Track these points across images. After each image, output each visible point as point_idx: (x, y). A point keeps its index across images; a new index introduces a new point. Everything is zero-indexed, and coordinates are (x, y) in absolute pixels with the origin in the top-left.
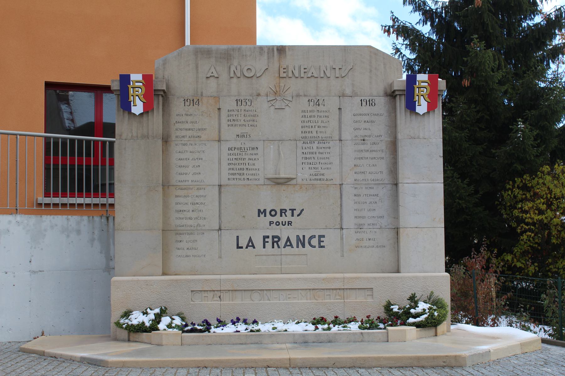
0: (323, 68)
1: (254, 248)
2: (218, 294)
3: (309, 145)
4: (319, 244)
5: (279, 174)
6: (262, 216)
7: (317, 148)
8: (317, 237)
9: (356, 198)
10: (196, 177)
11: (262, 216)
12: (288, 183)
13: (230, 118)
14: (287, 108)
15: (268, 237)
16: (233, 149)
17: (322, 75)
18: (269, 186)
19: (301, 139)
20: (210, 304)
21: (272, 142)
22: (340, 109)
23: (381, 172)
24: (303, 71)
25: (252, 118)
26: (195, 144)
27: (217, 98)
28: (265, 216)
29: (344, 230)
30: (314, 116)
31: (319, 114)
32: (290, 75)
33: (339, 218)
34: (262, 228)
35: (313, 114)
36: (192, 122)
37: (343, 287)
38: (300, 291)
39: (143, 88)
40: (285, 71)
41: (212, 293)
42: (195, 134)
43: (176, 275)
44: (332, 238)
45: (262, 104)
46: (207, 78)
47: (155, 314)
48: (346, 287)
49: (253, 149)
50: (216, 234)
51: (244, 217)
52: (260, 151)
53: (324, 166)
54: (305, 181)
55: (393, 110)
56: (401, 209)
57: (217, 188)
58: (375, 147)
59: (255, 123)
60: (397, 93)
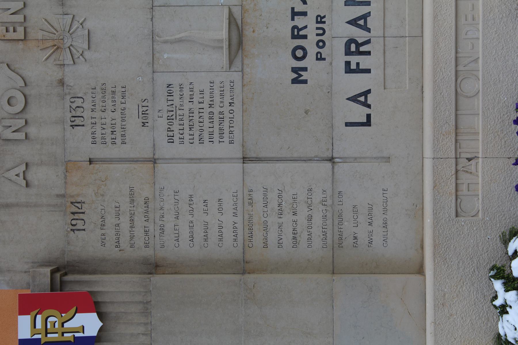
1: (369, 91)
2: (463, 162)
5: (221, 41)
6: (305, 75)
10: (228, 205)
11: (305, 75)
12: (239, 22)
13: (108, 140)
14: (88, 25)
15: (348, 64)
16: (171, 134)
18: (246, 61)
20: (483, 179)
21: (157, 55)
25: (108, 96)
26: (162, 208)
27: (69, 166)
28: (305, 69)
32: (19, 18)
34: (329, 74)
36: (118, 215)
39: (47, 312)
40: (11, 29)
41: (461, 175)
42: (141, 209)
43: (422, 247)
45: (80, 76)
46: (27, 185)
47: (507, 291)
49: (170, 94)
50: (342, 168)
51: (306, 112)
52: (176, 80)
57: (249, 166)
59: (119, 89)
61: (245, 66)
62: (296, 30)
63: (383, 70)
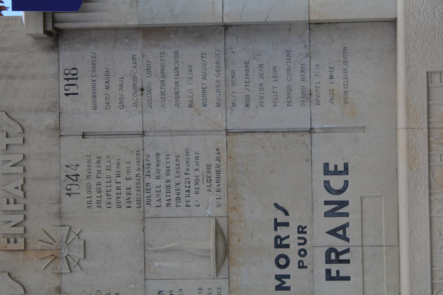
0: (7, 168)
3: (153, 193)
4: (340, 173)
5: (208, 251)
7: (158, 178)
8: (328, 178)
9: (252, 104)
11: (288, 283)
12: (225, 232)
14: (84, 235)
15: (328, 271)
17: (20, 169)
18: (232, 269)
19: (141, 209)
21: (148, 264)
22: (84, 135)
23: (203, 56)
24: (12, 207)
28: (288, 277)
29: (315, 126)
30: (99, 184)
31: (94, 174)
32: (20, 230)
33: (291, 135)
35: (94, 186)
37: (426, 130)
38: (434, 214)
40: (12, 240)
44: (329, 151)
48: (425, 125)
53: (193, 165)
54: (223, 201)
55: (86, 35)
56: (272, 18)
58: (156, 68)
60: (50, 28)
61: (231, 274)
62: (279, 240)
63: (362, 278)
